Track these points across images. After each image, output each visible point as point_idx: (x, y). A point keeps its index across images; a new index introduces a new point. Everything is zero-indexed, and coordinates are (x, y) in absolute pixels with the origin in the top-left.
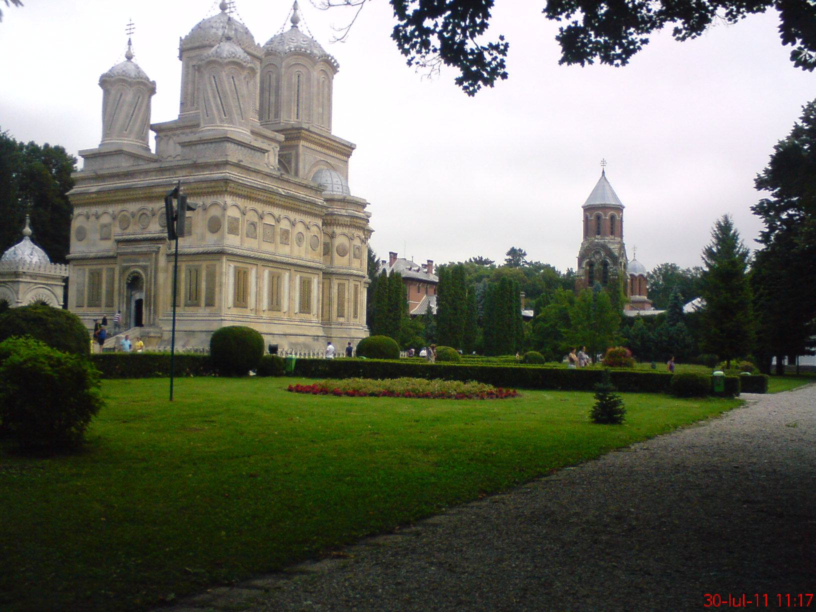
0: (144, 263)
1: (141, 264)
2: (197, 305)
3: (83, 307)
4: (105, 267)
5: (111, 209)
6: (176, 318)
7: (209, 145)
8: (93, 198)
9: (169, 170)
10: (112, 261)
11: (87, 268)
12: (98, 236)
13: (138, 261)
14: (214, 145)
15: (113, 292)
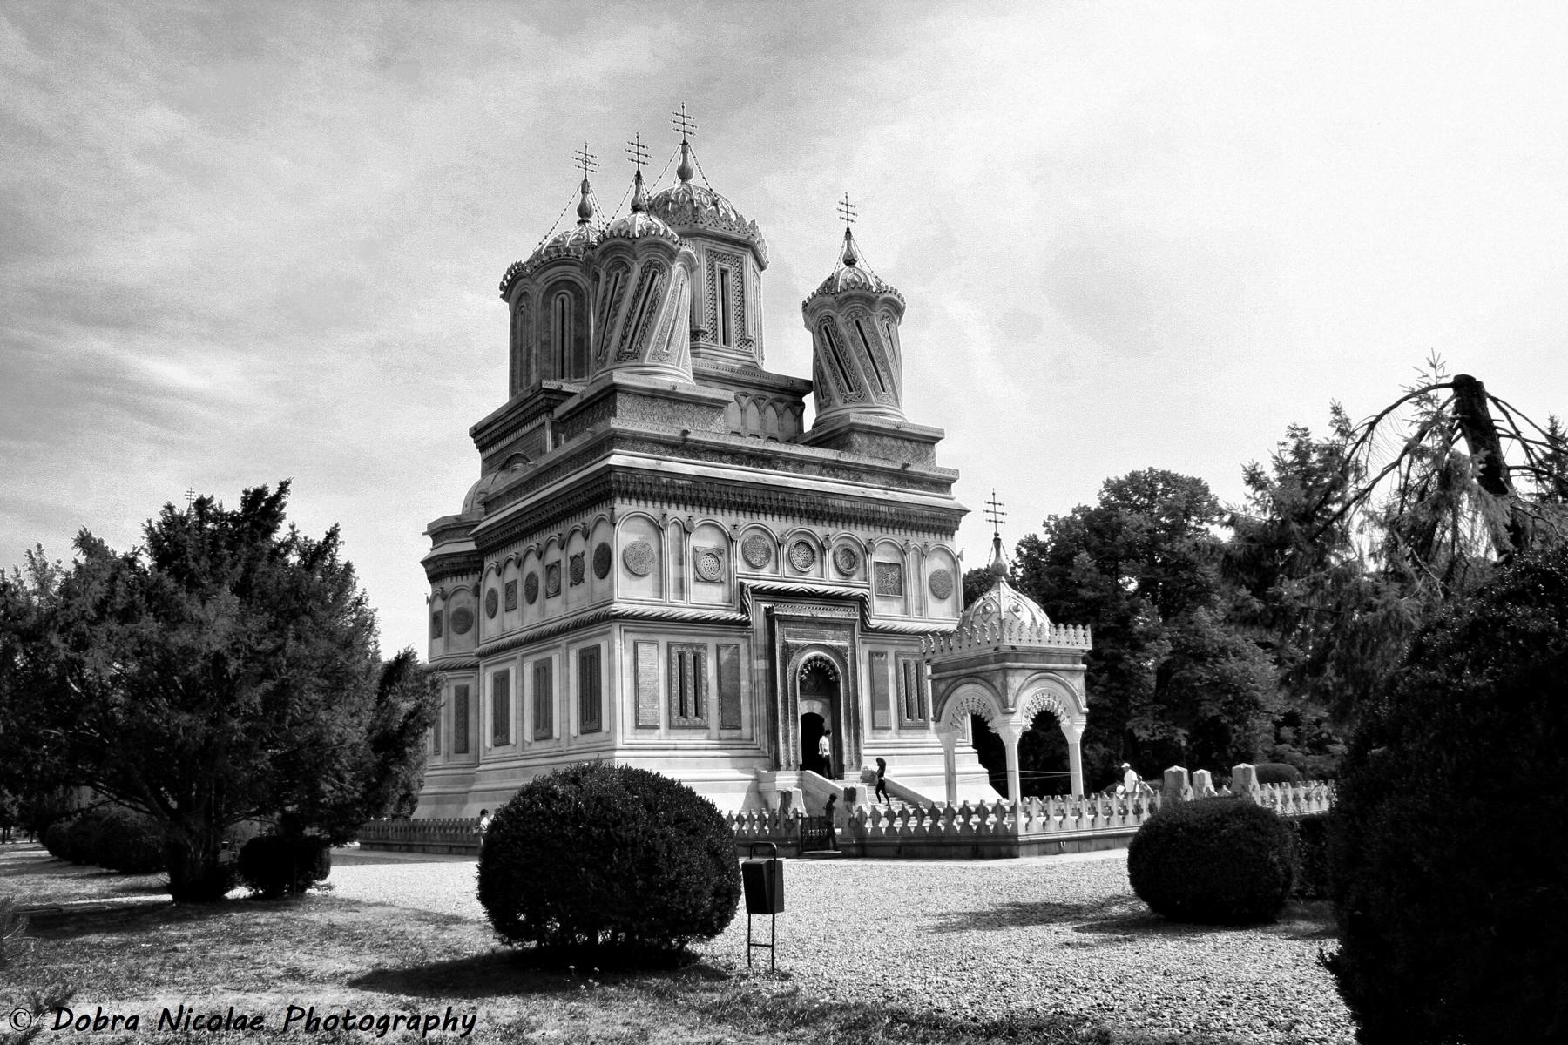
0: (834, 643)
1: (828, 642)
2: (925, 727)
3: (657, 728)
4: (711, 643)
5: (725, 519)
6: (864, 752)
7: (907, 444)
8: (681, 487)
9: (848, 470)
10: (735, 630)
11: (663, 641)
12: (690, 573)
13: (823, 638)
14: (914, 445)
15: (739, 697)
